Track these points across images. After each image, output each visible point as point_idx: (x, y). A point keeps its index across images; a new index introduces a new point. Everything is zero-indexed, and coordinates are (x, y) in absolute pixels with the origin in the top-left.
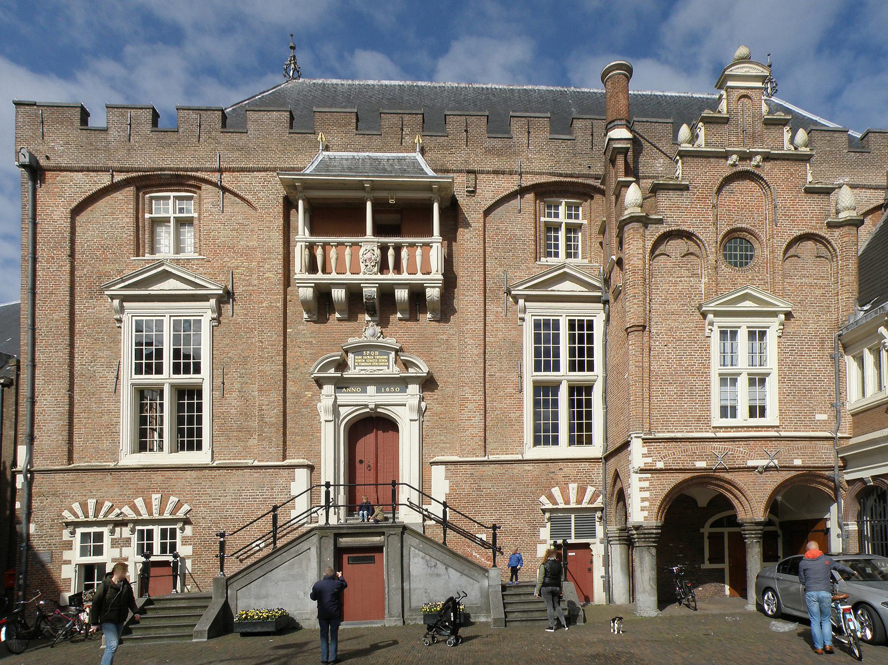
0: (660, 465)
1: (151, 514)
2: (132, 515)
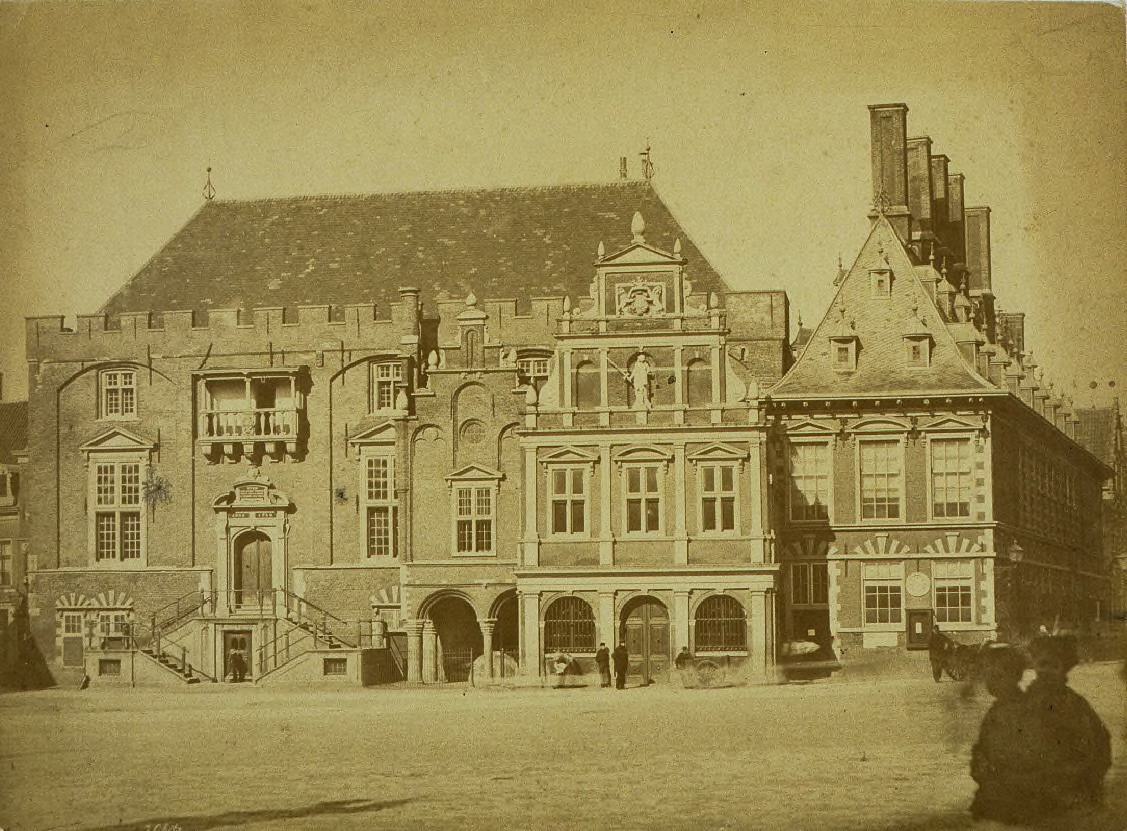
0: (418, 582)
1: (108, 604)
2: (97, 606)
